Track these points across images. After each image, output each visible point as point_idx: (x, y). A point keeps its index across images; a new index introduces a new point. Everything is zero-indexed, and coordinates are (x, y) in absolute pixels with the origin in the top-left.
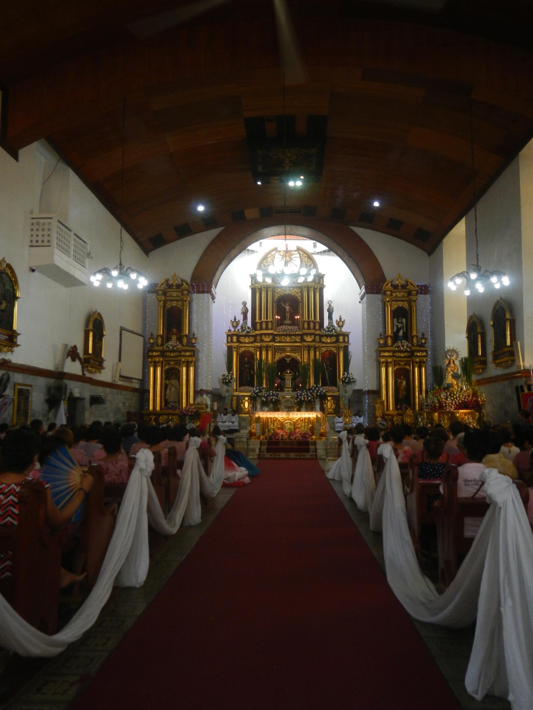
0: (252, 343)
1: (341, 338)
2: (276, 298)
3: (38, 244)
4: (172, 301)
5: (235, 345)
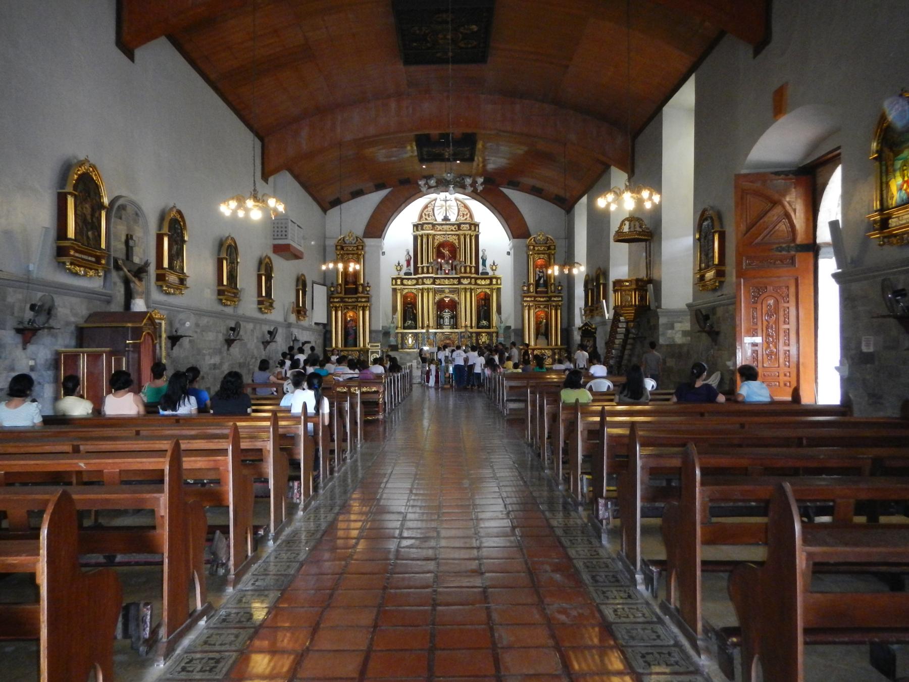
0: (414, 285)
1: (494, 281)
2: (436, 244)
3: (278, 237)
4: (348, 254)
5: (399, 287)
